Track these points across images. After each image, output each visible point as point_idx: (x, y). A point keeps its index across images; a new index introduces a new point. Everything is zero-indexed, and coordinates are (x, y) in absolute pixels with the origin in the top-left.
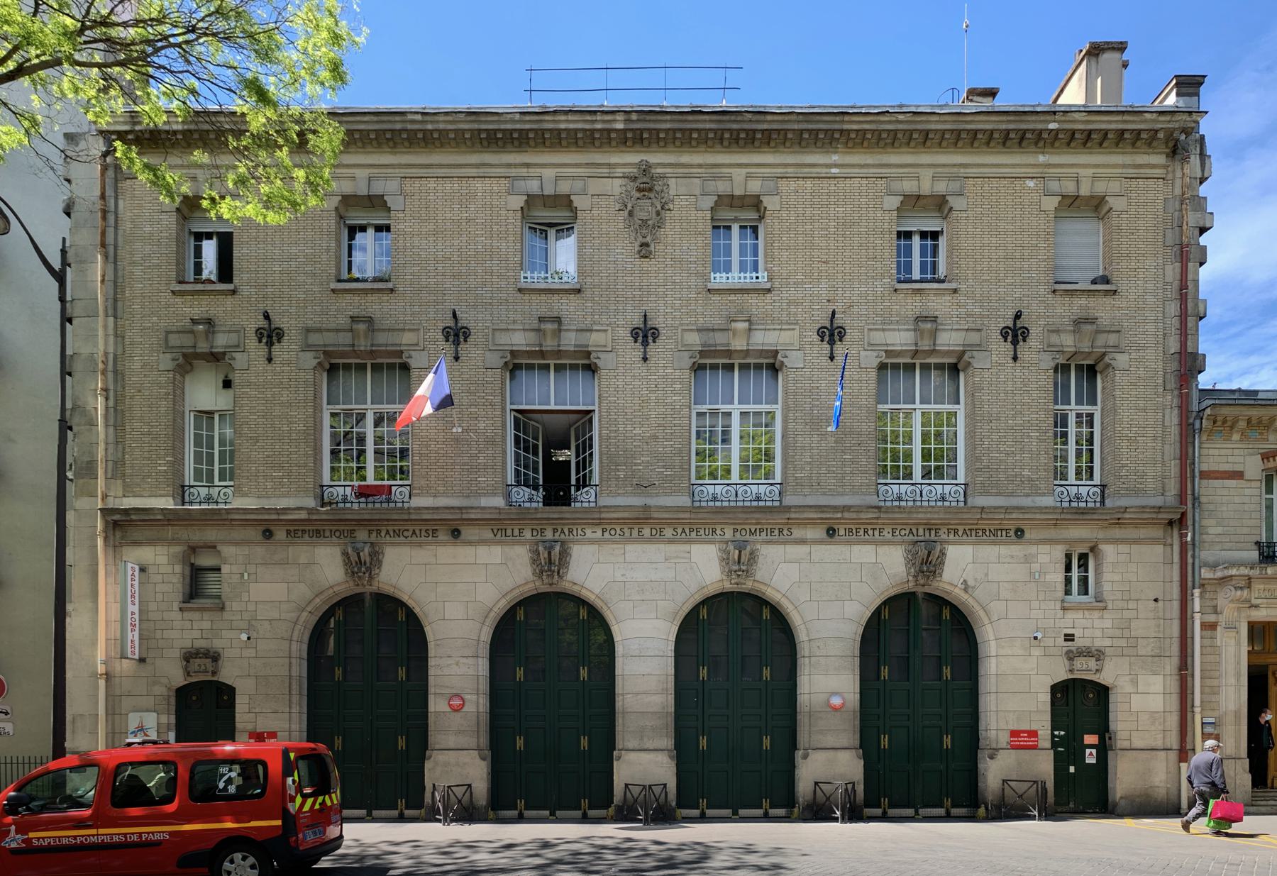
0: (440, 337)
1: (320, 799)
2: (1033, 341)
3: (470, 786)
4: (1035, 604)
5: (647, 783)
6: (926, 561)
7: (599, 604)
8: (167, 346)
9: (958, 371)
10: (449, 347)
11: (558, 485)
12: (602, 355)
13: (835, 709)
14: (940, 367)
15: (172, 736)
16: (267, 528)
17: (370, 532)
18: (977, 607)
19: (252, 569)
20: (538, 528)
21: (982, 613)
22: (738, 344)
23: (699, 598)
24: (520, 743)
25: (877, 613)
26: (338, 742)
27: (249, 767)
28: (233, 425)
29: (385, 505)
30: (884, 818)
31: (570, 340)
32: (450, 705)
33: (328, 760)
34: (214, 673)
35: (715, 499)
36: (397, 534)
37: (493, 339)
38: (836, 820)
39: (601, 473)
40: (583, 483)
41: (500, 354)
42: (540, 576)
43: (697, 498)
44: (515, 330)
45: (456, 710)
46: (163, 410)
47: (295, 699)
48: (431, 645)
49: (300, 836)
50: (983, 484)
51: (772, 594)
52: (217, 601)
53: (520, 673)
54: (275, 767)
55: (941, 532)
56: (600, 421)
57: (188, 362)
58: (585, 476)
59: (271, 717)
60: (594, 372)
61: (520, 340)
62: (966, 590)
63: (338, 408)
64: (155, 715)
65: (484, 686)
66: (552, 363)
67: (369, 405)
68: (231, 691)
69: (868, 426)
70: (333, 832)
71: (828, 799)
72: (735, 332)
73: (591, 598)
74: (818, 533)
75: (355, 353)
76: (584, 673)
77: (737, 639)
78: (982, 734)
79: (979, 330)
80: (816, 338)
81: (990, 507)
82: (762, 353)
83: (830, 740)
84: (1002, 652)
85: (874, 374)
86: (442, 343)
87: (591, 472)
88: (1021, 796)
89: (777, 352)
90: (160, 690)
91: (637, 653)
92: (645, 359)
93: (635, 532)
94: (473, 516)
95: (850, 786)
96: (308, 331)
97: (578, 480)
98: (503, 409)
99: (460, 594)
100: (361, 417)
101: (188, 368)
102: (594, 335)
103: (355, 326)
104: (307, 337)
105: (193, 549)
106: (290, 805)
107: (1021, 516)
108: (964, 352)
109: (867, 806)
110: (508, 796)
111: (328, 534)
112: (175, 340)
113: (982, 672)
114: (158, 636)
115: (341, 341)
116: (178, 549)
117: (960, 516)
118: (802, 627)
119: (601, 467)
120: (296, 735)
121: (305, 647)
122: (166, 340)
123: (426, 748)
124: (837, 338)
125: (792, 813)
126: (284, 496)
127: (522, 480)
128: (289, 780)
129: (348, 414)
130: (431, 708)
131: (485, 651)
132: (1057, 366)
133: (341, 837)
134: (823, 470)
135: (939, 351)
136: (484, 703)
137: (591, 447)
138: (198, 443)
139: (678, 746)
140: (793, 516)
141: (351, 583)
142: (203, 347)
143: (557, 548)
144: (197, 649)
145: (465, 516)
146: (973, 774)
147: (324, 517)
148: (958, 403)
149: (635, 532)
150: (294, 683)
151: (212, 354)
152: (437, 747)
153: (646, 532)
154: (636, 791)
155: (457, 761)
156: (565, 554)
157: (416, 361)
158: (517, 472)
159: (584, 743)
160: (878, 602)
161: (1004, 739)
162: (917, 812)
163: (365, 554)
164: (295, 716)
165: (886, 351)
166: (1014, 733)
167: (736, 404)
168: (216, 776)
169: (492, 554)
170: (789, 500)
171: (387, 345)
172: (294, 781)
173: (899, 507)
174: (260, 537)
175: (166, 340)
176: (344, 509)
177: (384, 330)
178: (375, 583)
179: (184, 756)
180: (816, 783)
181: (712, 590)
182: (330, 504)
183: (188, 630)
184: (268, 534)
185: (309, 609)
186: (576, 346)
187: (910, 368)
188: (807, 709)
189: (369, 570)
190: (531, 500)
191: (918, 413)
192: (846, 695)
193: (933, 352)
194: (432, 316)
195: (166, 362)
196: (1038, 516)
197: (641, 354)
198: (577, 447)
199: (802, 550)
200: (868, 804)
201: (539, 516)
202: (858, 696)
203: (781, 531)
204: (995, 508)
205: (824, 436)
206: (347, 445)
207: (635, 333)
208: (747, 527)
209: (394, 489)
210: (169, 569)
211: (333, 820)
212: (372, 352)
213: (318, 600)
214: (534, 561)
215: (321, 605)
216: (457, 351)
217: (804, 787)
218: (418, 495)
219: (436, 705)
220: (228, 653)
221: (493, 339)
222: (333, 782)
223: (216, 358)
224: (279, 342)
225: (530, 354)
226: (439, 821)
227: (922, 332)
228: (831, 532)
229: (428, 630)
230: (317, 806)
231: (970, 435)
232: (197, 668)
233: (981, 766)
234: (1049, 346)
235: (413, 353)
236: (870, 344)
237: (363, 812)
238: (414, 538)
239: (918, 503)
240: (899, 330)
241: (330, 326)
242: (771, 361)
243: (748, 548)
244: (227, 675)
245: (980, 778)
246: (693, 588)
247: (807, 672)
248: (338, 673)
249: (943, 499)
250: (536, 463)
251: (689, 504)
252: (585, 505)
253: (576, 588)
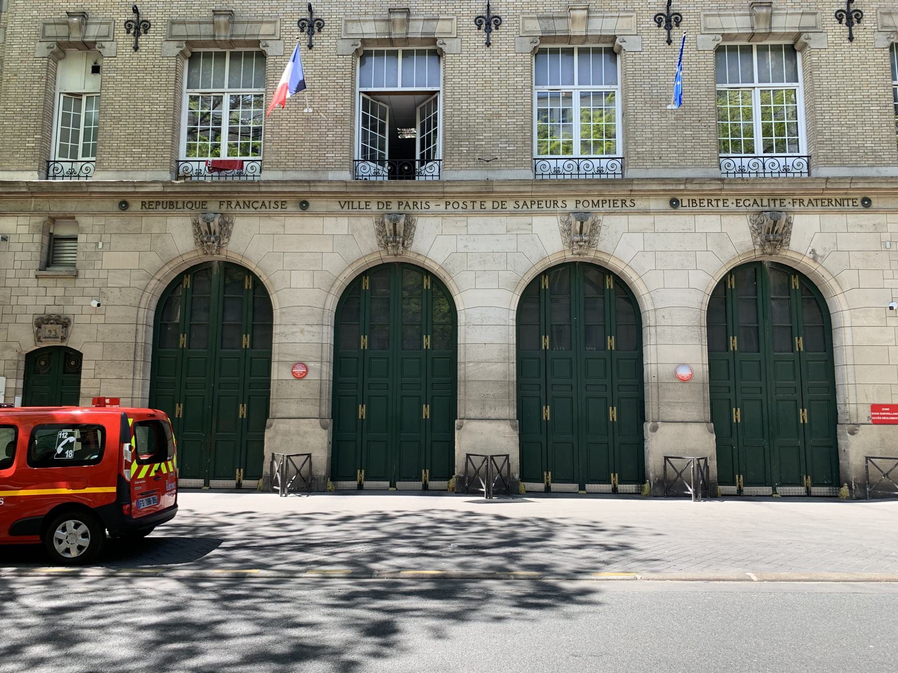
0: (296, 27)
1: (156, 466)
2: (868, 21)
3: (309, 455)
4: (888, 274)
5: (489, 454)
6: (772, 230)
7: (441, 274)
8: (44, 36)
9: (795, 51)
10: (304, 37)
11: (403, 161)
12: (447, 41)
13: (684, 381)
14: (776, 49)
15: (18, 401)
16: (123, 200)
17: (221, 203)
18: (828, 277)
19: (106, 238)
20: (384, 201)
21: (832, 283)
22: (578, 30)
23: (540, 268)
24: (362, 411)
25: (723, 282)
26: (179, 410)
27: (89, 432)
28: (98, 106)
29: (236, 179)
30: (739, 496)
31: (417, 29)
32: (293, 373)
33: (167, 428)
34: (63, 339)
35: (557, 172)
36: (247, 205)
37: (346, 30)
38: (688, 497)
39: (444, 149)
40: (427, 158)
41: (352, 42)
42: (386, 247)
43: (539, 172)
44: (365, 21)
45: (299, 378)
46: (35, 91)
47: (140, 365)
48: (276, 313)
49: (134, 504)
50: (826, 157)
51: (615, 264)
52: (71, 269)
53: (364, 341)
54: (113, 433)
55: (786, 202)
56: (444, 100)
57: (61, 50)
58: (429, 151)
59: (115, 382)
60: (439, 57)
61: (371, 30)
62: (814, 259)
63: (196, 92)
64: (4, 379)
65: (328, 354)
66: (400, 49)
67: (226, 89)
68: (78, 356)
69: (708, 104)
70: (167, 501)
71: (679, 475)
72: (574, 20)
73: (434, 268)
74: (663, 204)
75: (216, 43)
76: (427, 341)
77: (582, 310)
78: (841, 409)
79: (815, 14)
80: (653, 24)
81: (834, 178)
82: (600, 38)
83: (679, 413)
84: (856, 322)
85: (712, 56)
86: (297, 33)
87: (435, 148)
88: (886, 475)
89: (615, 37)
90: (11, 355)
91: (478, 322)
92: (488, 44)
93: (477, 205)
94: (321, 189)
95: (702, 462)
96: (173, 23)
97: (422, 156)
98: (353, 91)
99: (305, 264)
100: (218, 101)
101: (62, 55)
102: (440, 23)
103: (216, 19)
104: (171, 29)
105: (53, 220)
106: (125, 472)
107: (867, 186)
108: (800, 34)
109: (721, 483)
110: (346, 469)
111: (180, 205)
112: (51, 31)
113: (836, 342)
114: (13, 302)
115: (203, 32)
116: (38, 220)
117: (804, 186)
118: (647, 296)
119: (445, 143)
120: (138, 401)
121: (152, 314)
122: (44, 30)
123: (267, 416)
124: (673, 23)
125: (642, 489)
126: (145, 169)
127: (368, 155)
128: (126, 446)
129: (205, 98)
130: (274, 376)
131: (330, 319)
132: (892, 44)
133: (175, 506)
134: (664, 145)
135: (774, 34)
136: (327, 371)
137: (435, 125)
138: (65, 122)
139: (521, 415)
140: (635, 188)
141: (200, 252)
142: (76, 36)
143: (402, 221)
144: (50, 315)
145: (313, 189)
146: (833, 452)
147: (178, 190)
148: (797, 81)
149: (477, 205)
150: (139, 349)
151: (84, 42)
152: (278, 415)
153: (488, 205)
154: (478, 461)
155: (298, 429)
156: (409, 226)
157: (273, 49)
158: (364, 149)
159: (426, 411)
160: (724, 271)
161: (865, 414)
162: (774, 490)
163: (215, 225)
164: (138, 383)
165: (723, 35)
166: (875, 408)
167: (575, 83)
168: (53, 440)
169: (338, 226)
170: (630, 173)
171: (245, 36)
172: (131, 447)
173: (743, 179)
174: (116, 208)
175: (44, 30)
176: (197, 182)
177: (243, 22)
178: (223, 252)
179: (23, 419)
180: (666, 458)
181: (554, 260)
182: (185, 177)
183: (39, 297)
184: (124, 206)
185: (158, 277)
186: (422, 33)
187: (747, 50)
188: (655, 380)
189: (219, 239)
190: (376, 174)
191: (758, 91)
192: (694, 367)
193: (769, 35)
194: (288, 9)
195: (42, 49)
196: (885, 186)
197: (484, 40)
198: (422, 125)
199: (647, 220)
200: (722, 481)
201: (384, 190)
202: (706, 367)
203: (624, 202)
204: (840, 178)
205: (664, 113)
206: (204, 127)
207: (478, 21)
208: (589, 199)
209: (245, 164)
210: (28, 238)
211: (169, 487)
212: (231, 41)
213: (167, 268)
214: (380, 233)
215: (170, 273)
216: (311, 40)
217: (653, 462)
218: (269, 169)
219: (279, 373)
220: (78, 319)
221: (346, 30)
222: (170, 450)
223: (87, 46)
224: (146, 32)
225: (379, 42)
226: (276, 491)
227: (758, 16)
228: (675, 203)
229: (274, 299)
230: (152, 474)
231: (811, 110)
232: (47, 334)
233: (841, 442)
234: (883, 27)
235: (269, 42)
236: (706, 29)
237: (200, 482)
238: (263, 209)
239: (762, 175)
240: (735, 15)
241: (193, 19)
242: (610, 45)
243: (590, 219)
244: (75, 341)
245: (841, 455)
246: (535, 259)
247: (653, 341)
248: (183, 339)
249: (786, 171)
250: (382, 141)
251: (532, 177)
252: (429, 178)
253: (420, 259)
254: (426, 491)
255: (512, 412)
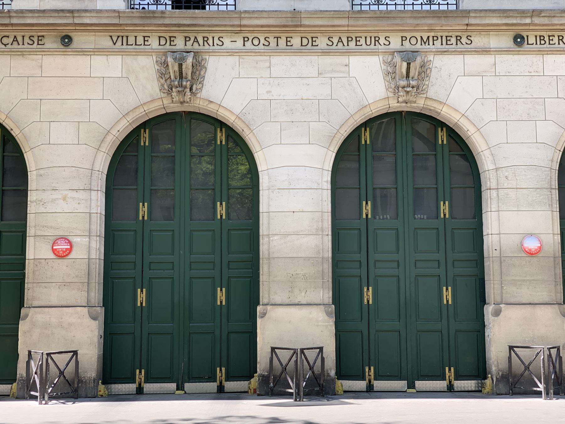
3: (75, 353)
5: (299, 347)
7: (239, 126)
13: (531, 254)
20: (167, 35)
23: (359, 119)
24: (141, 297)
32: (54, 251)
45: (61, 255)
53: (143, 210)
65: (98, 226)
71: (527, 368)
73: (230, 119)
74: (505, 41)
76: (221, 210)
83: (526, 294)
93: (282, 42)
94: (87, 21)
95: (554, 352)
118: (487, 153)
123: (21, 304)
125: (483, 385)
130: (30, 254)
131: (100, 182)
136: (97, 247)
139: (337, 299)
140: (472, 21)
143: (190, 60)
145: (77, 21)
149: (282, 42)
152: (36, 303)
153: (296, 41)
154: (284, 356)
156: (199, 66)
169: (110, 66)
180: (511, 348)
188: (496, 254)
192: (542, 237)
201: (167, 21)
202: (558, 238)
203: (458, 39)
208: (418, 35)
217: (496, 354)
219: (36, 250)
226: (34, 398)
228: (519, 40)
238: (15, 45)
243: (419, 60)
246: (353, 109)
247: (494, 207)
254: (221, 393)
255: (326, 295)
